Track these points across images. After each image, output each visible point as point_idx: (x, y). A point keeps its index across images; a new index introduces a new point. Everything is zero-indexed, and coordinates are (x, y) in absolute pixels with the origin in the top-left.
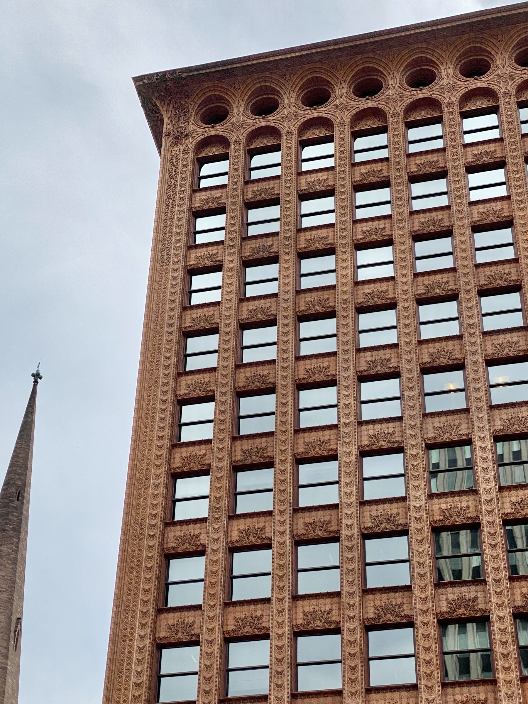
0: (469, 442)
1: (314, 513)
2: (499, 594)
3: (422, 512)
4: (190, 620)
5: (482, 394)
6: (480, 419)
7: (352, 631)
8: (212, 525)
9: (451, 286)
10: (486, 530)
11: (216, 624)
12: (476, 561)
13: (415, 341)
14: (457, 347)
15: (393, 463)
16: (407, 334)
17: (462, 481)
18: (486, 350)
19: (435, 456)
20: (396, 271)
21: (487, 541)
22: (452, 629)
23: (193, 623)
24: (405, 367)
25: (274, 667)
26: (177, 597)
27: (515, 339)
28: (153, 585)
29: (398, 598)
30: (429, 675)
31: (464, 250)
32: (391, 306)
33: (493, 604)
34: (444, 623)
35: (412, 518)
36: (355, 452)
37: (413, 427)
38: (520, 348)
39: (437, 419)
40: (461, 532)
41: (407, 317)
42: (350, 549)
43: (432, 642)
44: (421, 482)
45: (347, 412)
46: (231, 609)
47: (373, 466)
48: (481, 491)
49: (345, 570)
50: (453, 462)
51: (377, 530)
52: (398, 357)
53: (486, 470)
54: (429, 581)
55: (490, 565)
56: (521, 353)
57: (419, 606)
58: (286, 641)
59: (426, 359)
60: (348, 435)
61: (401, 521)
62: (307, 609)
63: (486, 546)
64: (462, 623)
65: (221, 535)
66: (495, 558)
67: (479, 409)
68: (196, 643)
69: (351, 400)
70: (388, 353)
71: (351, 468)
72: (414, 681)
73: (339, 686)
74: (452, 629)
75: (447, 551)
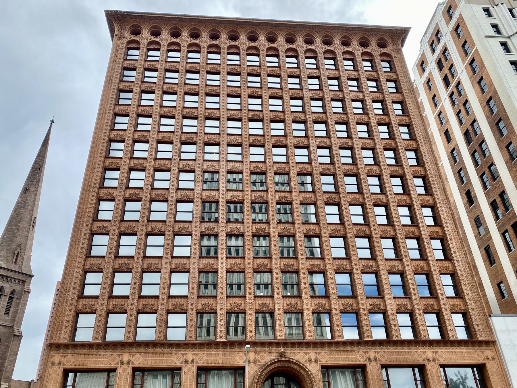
0: (218, 172)
2: (222, 227)
3: (199, 195)
4: (106, 225)
5: (225, 156)
6: (223, 165)
7: (169, 235)
8: (118, 190)
10: (221, 204)
11: (117, 228)
12: (216, 215)
13: (203, 133)
14: (218, 138)
17: (214, 186)
19: (207, 176)
23: (107, 227)
24: (198, 141)
25: (137, 246)
26: (102, 216)
28: (92, 210)
29: (187, 225)
31: (223, 103)
34: (202, 235)
36: (177, 170)
37: (199, 164)
42: (171, 205)
44: (200, 184)
46: (123, 223)
47: (183, 176)
48: (221, 190)
50: (212, 179)
53: (223, 183)
54: (199, 220)
55: (220, 217)
57: (194, 229)
58: (143, 237)
59: (206, 140)
62: (153, 226)
63: (220, 210)
64: (209, 236)
65: (122, 194)
67: (223, 161)
68: (108, 234)
69: (177, 150)
73: (161, 255)
74: (206, 238)
75: (207, 210)
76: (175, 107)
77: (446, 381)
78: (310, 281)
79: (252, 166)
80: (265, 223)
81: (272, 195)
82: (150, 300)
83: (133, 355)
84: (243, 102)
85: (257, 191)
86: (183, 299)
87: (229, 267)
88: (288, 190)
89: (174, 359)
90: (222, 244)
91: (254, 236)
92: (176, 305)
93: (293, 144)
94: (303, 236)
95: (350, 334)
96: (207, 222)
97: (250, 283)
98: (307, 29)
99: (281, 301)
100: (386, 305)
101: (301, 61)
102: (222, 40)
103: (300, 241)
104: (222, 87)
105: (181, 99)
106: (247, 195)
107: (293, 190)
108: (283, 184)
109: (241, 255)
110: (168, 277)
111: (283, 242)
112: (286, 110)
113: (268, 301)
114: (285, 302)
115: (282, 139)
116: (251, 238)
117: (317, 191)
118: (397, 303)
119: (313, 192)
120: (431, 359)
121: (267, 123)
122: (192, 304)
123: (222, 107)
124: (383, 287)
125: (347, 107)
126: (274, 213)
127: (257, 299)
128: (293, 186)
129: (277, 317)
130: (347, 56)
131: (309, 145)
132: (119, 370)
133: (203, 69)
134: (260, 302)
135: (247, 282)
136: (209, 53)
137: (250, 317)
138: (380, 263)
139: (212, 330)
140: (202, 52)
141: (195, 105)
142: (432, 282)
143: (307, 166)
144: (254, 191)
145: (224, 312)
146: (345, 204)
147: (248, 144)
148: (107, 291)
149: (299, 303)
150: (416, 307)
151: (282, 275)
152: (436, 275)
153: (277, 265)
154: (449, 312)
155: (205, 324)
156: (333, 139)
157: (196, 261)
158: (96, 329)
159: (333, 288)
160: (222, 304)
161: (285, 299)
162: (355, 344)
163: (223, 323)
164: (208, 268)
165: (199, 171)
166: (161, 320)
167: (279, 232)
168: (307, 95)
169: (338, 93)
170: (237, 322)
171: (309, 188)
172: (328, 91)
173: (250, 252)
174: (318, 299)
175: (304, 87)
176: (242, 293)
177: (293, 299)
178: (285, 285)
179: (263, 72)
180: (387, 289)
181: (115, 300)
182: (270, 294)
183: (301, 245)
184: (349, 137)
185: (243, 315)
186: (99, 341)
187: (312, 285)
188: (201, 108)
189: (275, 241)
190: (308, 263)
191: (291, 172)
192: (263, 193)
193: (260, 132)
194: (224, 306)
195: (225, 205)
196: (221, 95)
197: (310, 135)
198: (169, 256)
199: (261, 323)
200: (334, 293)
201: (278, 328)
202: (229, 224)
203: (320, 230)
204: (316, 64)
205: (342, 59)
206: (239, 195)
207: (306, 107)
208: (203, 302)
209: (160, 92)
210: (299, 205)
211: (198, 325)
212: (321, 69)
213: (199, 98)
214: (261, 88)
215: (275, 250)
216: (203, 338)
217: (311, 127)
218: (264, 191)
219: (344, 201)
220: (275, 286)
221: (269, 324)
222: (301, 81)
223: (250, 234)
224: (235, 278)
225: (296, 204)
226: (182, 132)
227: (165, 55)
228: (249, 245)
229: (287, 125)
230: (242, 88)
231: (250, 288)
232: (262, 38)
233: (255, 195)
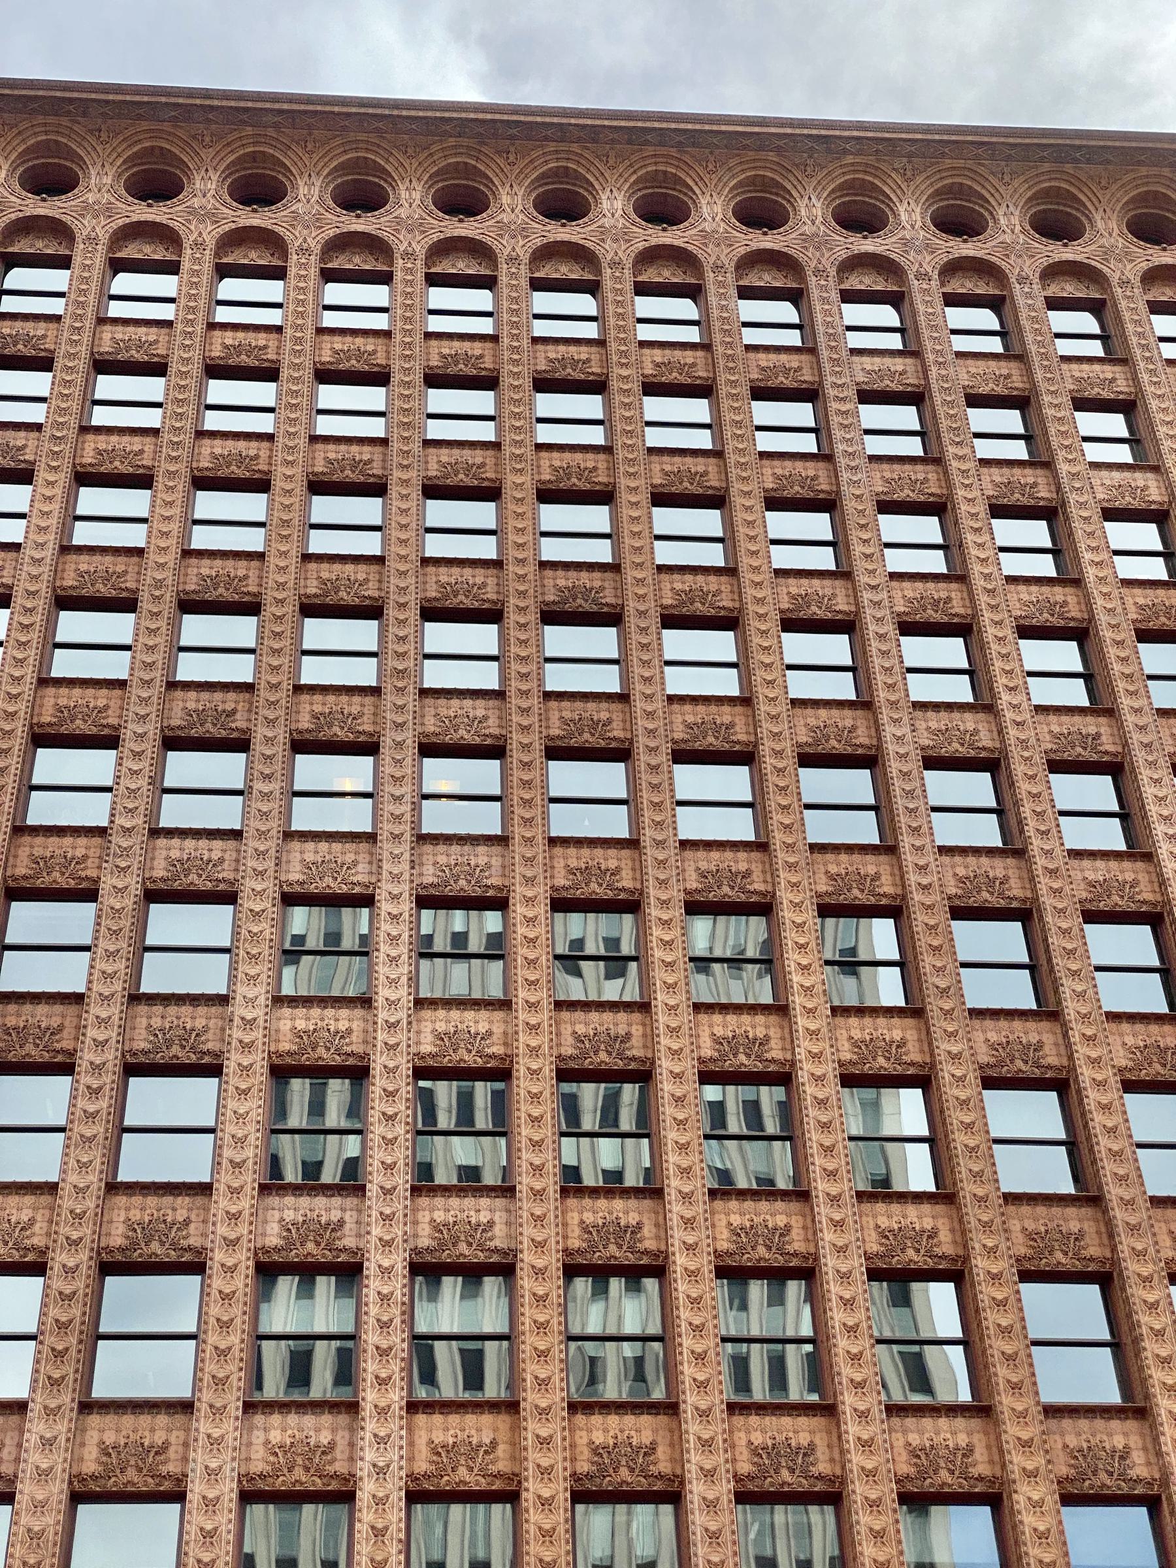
0: (367, 901)
1: (28, 1008)
2: (387, 1218)
3: (255, 1033)
6: (396, 858)
9: (371, 591)
10: (378, 1083)
12: (352, 1147)
15: (210, 924)
16: (275, 669)
17: (344, 977)
18: (423, 724)
19: (300, 919)
20: (268, 541)
21: (377, 1106)
24: (260, 732)
27: (480, 713)
30: (220, 1383)
31: (404, 527)
32: (250, 608)
33: (374, 1240)
34: (268, 1271)
35: (234, 1043)
36: (136, 889)
37: (260, 854)
38: (487, 732)
39: (310, 846)
40: (331, 1081)
41: (277, 635)
42: (95, 1092)
43: (237, 1310)
44: (261, 969)
45: (131, 806)
47: (169, 923)
48: (380, 1001)
49: (75, 1136)
50: (333, 937)
51: (158, 1058)
52: (250, 711)
53: (393, 960)
54: (249, 1179)
55: (377, 1156)
56: (489, 741)
57: (222, 1230)
59: (305, 722)
60: (126, 852)
61: (210, 1046)
63: (374, 1116)
64: (307, 1272)
66: (390, 1142)
67: (396, 837)
69: (143, 782)
70: (230, 700)
71: (122, 923)
72: (185, 1393)
74: (286, 1286)
75: (297, 1118)
76: (139, 552)
79: (559, 864)
80: (636, 1192)
81: (674, 1031)
84: (512, 523)
85: (586, 1006)
88: (767, 998)
90: (384, 1325)
91: (571, 1271)
93: (787, 745)
94: (860, 1274)
96: (296, 1189)
98: (849, 159)
101: (819, 318)
102: (403, 212)
104: (395, 445)
105: (176, 511)
106: (534, 1028)
107: (798, 1001)
108: (736, 962)
109: (492, 1390)
111: (744, 1307)
112: (745, 562)
115: (726, 715)
116: (553, 1285)
117: (935, 1005)
119: (913, 1010)
121: (644, 630)
123: (396, 549)
125: (1082, 546)
126: (691, 1136)
128: (796, 978)
130: (1069, 289)
131: (879, 747)
133: (296, 363)
136: (330, 276)
140: (292, 271)
141: (253, 540)
143: (870, 865)
144: (572, 1005)
146: (1100, 1084)
147: (538, 747)
156: (1009, 715)
157: (228, 1428)
165: (259, 894)
167: (723, 1245)
168: (859, 488)
169: (1028, 476)
171: (888, 988)
172: (969, 465)
173: (552, 1370)
175: (840, 448)
179: (618, 371)
183: (851, 1330)
184: (1101, 704)
188: (284, 554)
189: (695, 1301)
191: (785, 896)
192: (622, 1016)
193: (607, 680)
195: (406, 1090)
196: (394, 490)
197: (882, 695)
198: (67, 1398)
202: (424, 1201)
203: (962, 1233)
204: (901, 330)
205: (1040, 303)
206: (482, 1028)
207: (858, 549)
209: (63, 478)
210: (832, 1088)
212: (930, 357)
213: (271, 502)
214: (607, 449)
215: (700, 1357)
217: (885, 654)
218: (628, 1006)
219: (1095, 1062)
222: (822, 416)
223: (552, 1261)
225: (819, 1079)
226: (172, 685)
227: (94, 287)
228: (542, 1327)
229: (756, 640)
230: (508, 450)
232: (613, 206)
233: (581, 1029)
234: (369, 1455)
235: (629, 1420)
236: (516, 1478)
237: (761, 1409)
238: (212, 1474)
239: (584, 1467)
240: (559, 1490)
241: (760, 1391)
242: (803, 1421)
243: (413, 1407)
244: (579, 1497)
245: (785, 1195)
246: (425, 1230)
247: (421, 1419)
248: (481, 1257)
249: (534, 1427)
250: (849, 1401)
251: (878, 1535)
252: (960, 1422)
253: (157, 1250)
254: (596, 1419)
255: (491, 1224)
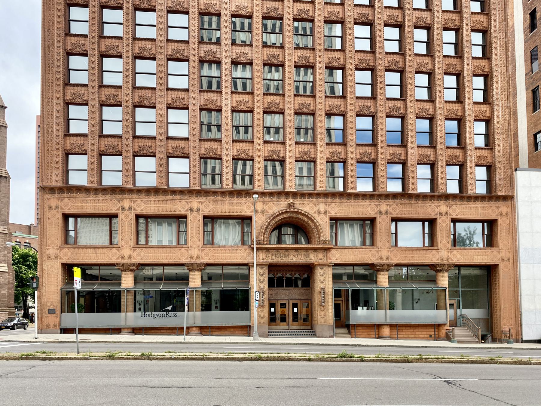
2: (226, 51)
22: (206, 65)
30: (194, 86)
33: (223, 56)
34: (202, 62)
43: (196, 70)
64: (210, 62)
72: (187, 88)
73: (154, 86)
74: (206, 65)
77: (454, 235)
78: (327, 126)
82: (147, 140)
83: (134, 202)
86: (183, 142)
87: (234, 105)
89: (178, 206)
90: (226, 75)
91: (265, 65)
92: (176, 148)
94: (323, 68)
95: (365, 186)
96: (207, 43)
97: (259, 125)
99: (292, 148)
100: (407, 155)
103: (320, 74)
109: (248, 90)
110: (164, 115)
111: (299, 75)
113: (279, 147)
114: (297, 150)
118: (420, 153)
120: (444, 213)
122: (194, 148)
124: (408, 134)
127: (266, 145)
129: (288, 165)
132: (121, 216)
134: (269, 149)
135: (255, 124)
137: (259, 164)
138: (409, 104)
139: (217, 177)
142: (463, 130)
145: (230, 158)
148: (96, 128)
149: (312, 150)
150: (440, 158)
151: (297, 117)
152: (469, 121)
153: (291, 104)
154: (473, 164)
155: (209, 171)
158: (90, 172)
159: (352, 134)
160: (227, 149)
161: (297, 146)
162: (368, 196)
163: (230, 170)
164: (211, 105)
166: (161, 165)
170: (244, 170)
173: (260, 86)
174: (334, 147)
176: (250, 138)
177: (306, 146)
178: (298, 129)
180: (412, 136)
181: (106, 139)
182: (281, 139)
183: (320, 80)
185: (251, 162)
186: (95, 185)
187: (328, 130)
189: (289, 72)
190: (327, 103)
194: (230, 152)
198: (164, 87)
199: (270, 172)
200: (352, 140)
201: (288, 177)
202: (234, 47)
203: (345, 59)
208: (206, 146)
211: (202, 172)
215: (290, 84)
216: (208, 186)
220: (288, 130)
221: (279, 173)
223: (260, 62)
224: (243, 119)
228: (258, 77)
231: (259, 132)
234: (224, 102)
235: (275, 97)
236: (253, 108)
237: (301, 96)
238: (194, 104)
239: (266, 106)
240: (261, 111)
241: (301, 92)
242: (309, 99)
243: (232, 93)
244: (265, 112)
245: (310, 49)
246: (234, 54)
247: (234, 95)
248: (246, 61)
249: (256, 98)
250: (318, 95)
251: (321, 121)
252: (339, 100)
253: (178, 56)
254: (269, 97)
255: (248, 53)
